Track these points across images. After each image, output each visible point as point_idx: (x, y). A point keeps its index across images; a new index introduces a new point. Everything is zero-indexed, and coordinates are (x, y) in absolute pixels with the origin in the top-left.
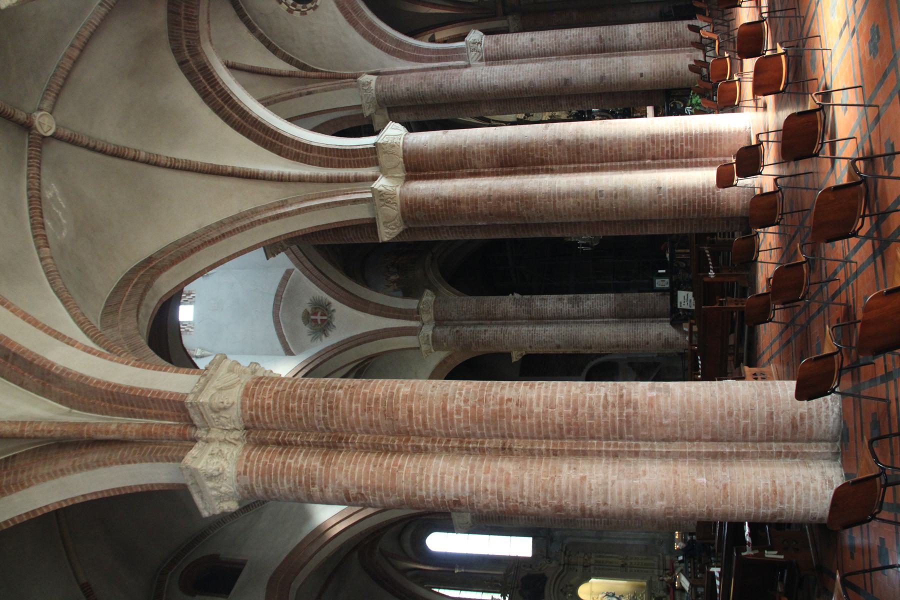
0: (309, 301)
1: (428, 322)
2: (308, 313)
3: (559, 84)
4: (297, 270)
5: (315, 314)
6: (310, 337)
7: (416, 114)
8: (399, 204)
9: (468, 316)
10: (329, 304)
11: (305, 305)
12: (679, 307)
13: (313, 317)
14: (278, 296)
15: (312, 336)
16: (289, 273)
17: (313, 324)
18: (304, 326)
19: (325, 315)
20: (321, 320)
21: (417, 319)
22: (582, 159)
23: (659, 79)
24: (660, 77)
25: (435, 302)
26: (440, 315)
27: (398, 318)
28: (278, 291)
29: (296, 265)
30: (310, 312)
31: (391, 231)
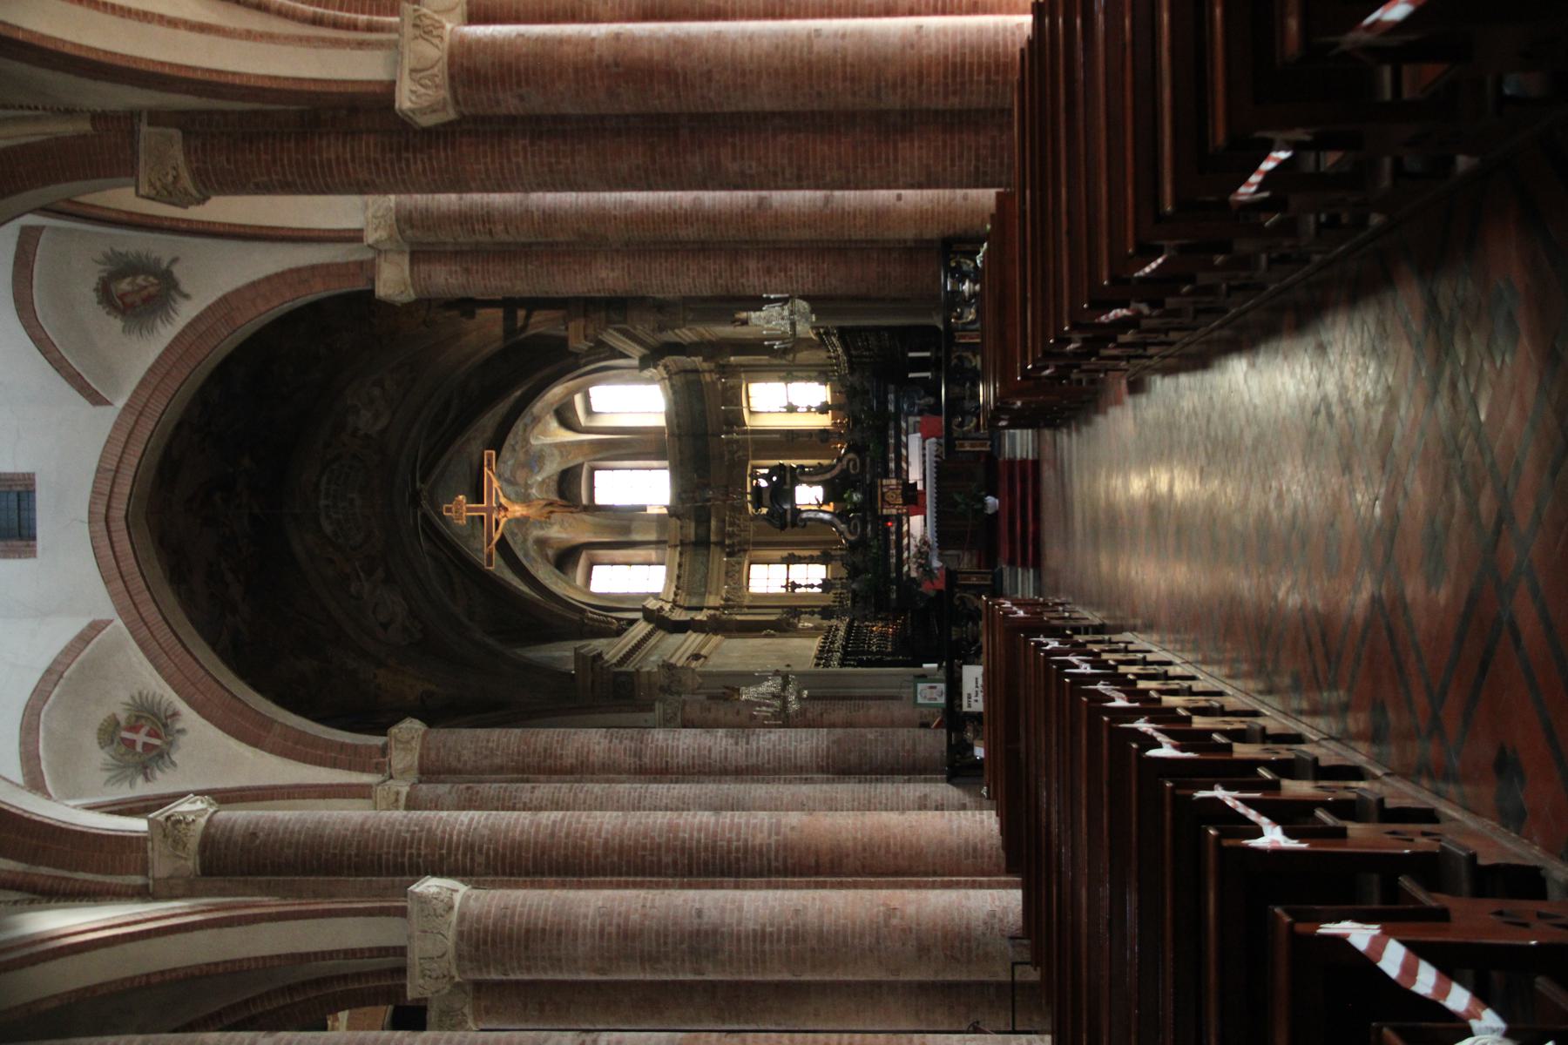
0: (127, 699)
1: (404, 772)
2: (118, 723)
3: (748, 206)
4: (119, 622)
5: (134, 728)
6: (106, 775)
7: (467, 271)
8: (447, 38)
9: (498, 761)
10: (175, 714)
11: (117, 704)
12: (965, 708)
14: (53, 674)
15: (112, 773)
16: (96, 628)
17: (123, 749)
18: (96, 746)
19: (157, 736)
20: (145, 745)
21: (378, 768)
22: (787, 10)
23: (930, 207)
24: (932, 201)
25: (425, 734)
26: (433, 755)
27: (335, 764)
28: (56, 662)
29: (121, 612)
30: (123, 723)
31: (422, 91)
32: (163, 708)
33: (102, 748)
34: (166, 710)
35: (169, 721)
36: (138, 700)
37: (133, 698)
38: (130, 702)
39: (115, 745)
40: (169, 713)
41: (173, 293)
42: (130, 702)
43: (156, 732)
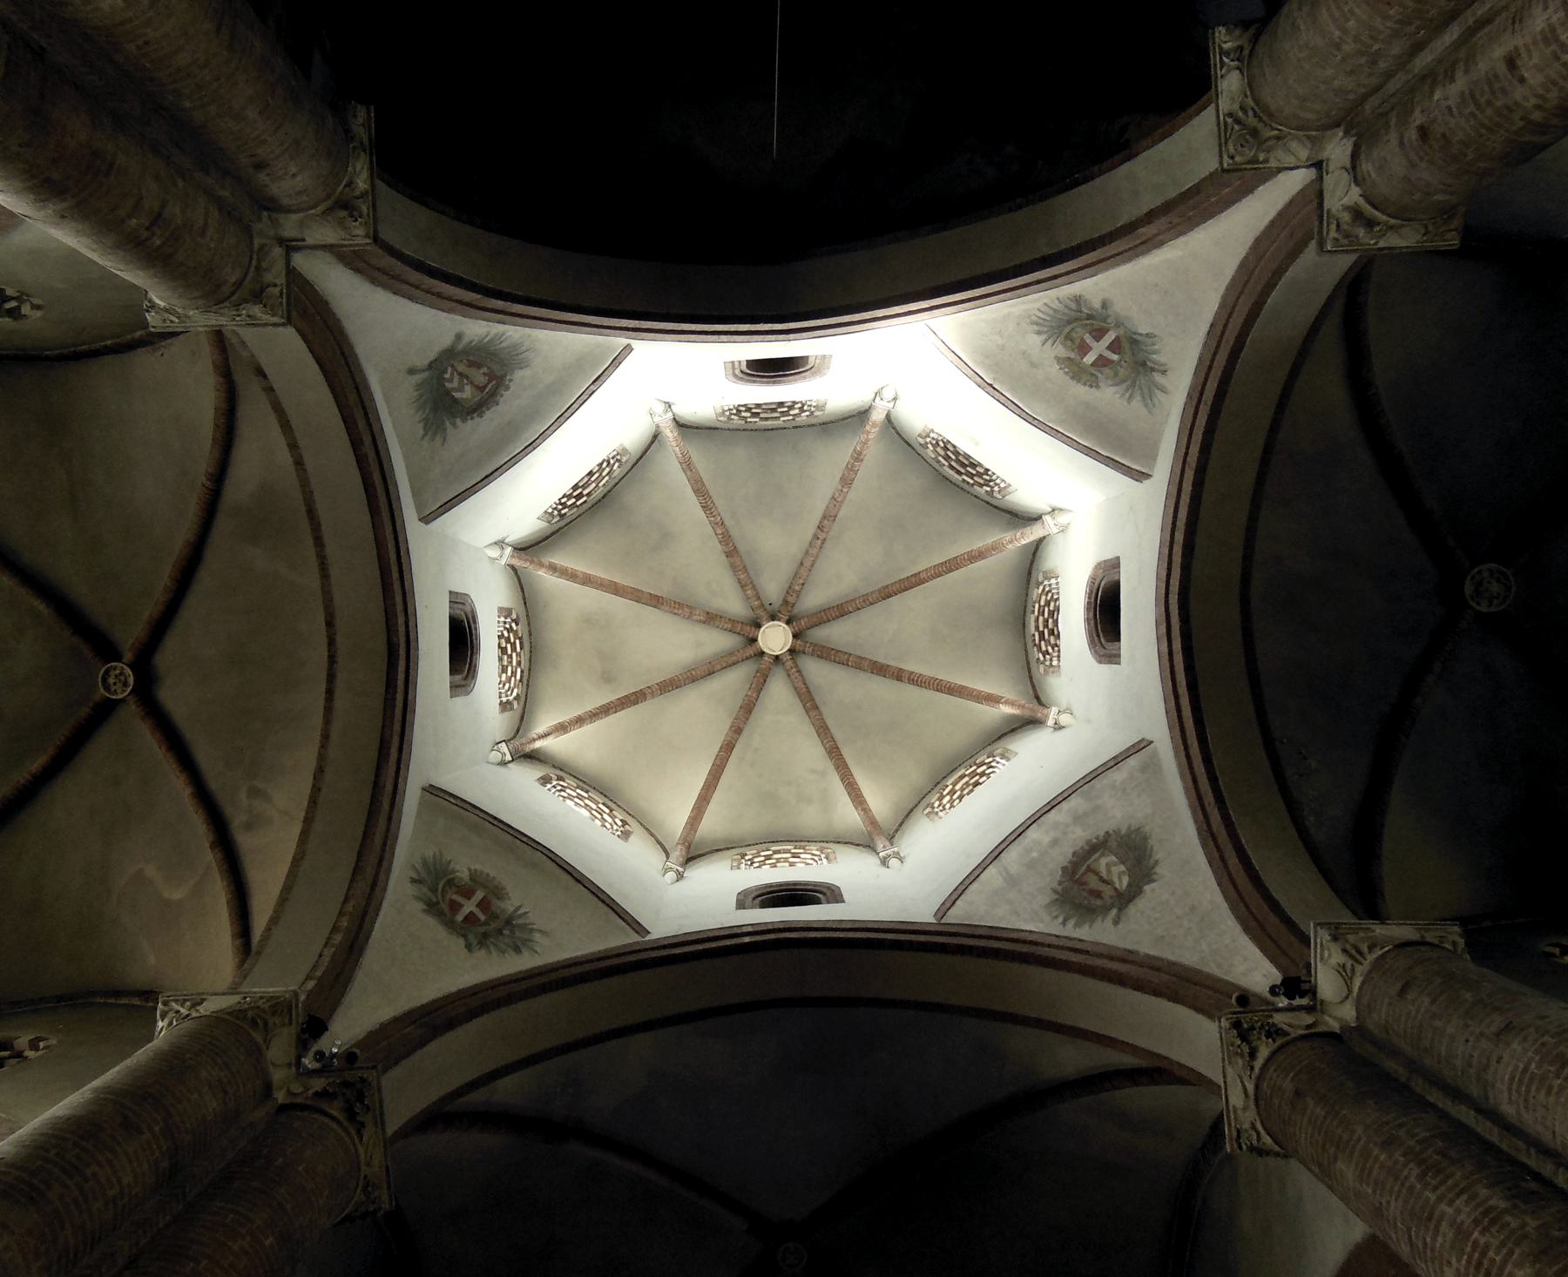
5: (1084, 349)
10: (1078, 300)
13: (1089, 359)
17: (1107, 370)
30: (1072, 355)
32: (1066, 311)
33: (1098, 387)
34: (1071, 309)
35: (1085, 311)
36: (1045, 329)
37: (1039, 333)
38: (1044, 337)
39: (1099, 375)
40: (1074, 306)
41: (460, 347)
42: (1044, 337)
43: (1096, 330)
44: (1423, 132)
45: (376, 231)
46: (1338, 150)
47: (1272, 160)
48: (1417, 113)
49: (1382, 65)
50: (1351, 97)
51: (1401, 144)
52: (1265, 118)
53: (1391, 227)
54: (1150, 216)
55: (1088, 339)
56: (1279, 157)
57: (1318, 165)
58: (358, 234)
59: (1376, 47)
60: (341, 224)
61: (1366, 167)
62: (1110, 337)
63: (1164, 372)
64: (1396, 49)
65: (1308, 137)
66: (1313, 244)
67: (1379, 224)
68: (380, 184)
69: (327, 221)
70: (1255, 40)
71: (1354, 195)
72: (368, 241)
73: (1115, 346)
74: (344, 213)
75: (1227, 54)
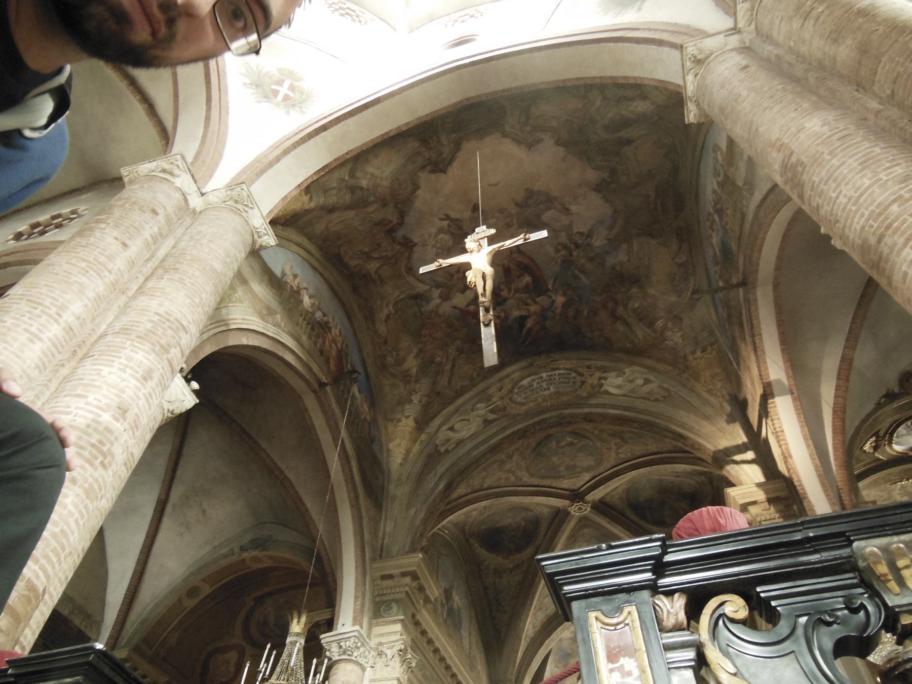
5: (292, 88)
13: (287, 83)
34: (305, 107)
35: (298, 109)
40: (304, 109)
43: (288, 100)
44: (155, 212)
45: (682, 52)
46: (196, 202)
47: (224, 192)
48: (163, 221)
49: (187, 237)
50: (197, 223)
51: (164, 208)
52: (235, 209)
53: (153, 171)
54: (278, 159)
55: (291, 94)
56: (222, 194)
57: (203, 194)
58: (691, 49)
59: (192, 243)
60: (701, 51)
61: (178, 195)
62: (280, 97)
63: (245, 84)
64: (183, 244)
65: (212, 205)
66: (190, 159)
67: (160, 171)
68: (682, 83)
69: (708, 50)
70: (254, 242)
71: (178, 182)
72: (686, 45)
73: (276, 93)
74: (699, 57)
75: (265, 234)
